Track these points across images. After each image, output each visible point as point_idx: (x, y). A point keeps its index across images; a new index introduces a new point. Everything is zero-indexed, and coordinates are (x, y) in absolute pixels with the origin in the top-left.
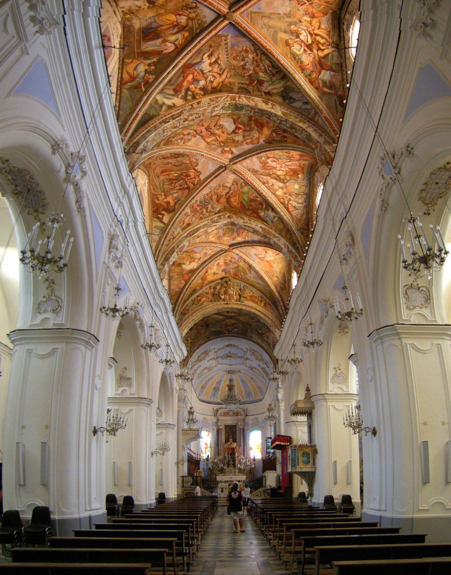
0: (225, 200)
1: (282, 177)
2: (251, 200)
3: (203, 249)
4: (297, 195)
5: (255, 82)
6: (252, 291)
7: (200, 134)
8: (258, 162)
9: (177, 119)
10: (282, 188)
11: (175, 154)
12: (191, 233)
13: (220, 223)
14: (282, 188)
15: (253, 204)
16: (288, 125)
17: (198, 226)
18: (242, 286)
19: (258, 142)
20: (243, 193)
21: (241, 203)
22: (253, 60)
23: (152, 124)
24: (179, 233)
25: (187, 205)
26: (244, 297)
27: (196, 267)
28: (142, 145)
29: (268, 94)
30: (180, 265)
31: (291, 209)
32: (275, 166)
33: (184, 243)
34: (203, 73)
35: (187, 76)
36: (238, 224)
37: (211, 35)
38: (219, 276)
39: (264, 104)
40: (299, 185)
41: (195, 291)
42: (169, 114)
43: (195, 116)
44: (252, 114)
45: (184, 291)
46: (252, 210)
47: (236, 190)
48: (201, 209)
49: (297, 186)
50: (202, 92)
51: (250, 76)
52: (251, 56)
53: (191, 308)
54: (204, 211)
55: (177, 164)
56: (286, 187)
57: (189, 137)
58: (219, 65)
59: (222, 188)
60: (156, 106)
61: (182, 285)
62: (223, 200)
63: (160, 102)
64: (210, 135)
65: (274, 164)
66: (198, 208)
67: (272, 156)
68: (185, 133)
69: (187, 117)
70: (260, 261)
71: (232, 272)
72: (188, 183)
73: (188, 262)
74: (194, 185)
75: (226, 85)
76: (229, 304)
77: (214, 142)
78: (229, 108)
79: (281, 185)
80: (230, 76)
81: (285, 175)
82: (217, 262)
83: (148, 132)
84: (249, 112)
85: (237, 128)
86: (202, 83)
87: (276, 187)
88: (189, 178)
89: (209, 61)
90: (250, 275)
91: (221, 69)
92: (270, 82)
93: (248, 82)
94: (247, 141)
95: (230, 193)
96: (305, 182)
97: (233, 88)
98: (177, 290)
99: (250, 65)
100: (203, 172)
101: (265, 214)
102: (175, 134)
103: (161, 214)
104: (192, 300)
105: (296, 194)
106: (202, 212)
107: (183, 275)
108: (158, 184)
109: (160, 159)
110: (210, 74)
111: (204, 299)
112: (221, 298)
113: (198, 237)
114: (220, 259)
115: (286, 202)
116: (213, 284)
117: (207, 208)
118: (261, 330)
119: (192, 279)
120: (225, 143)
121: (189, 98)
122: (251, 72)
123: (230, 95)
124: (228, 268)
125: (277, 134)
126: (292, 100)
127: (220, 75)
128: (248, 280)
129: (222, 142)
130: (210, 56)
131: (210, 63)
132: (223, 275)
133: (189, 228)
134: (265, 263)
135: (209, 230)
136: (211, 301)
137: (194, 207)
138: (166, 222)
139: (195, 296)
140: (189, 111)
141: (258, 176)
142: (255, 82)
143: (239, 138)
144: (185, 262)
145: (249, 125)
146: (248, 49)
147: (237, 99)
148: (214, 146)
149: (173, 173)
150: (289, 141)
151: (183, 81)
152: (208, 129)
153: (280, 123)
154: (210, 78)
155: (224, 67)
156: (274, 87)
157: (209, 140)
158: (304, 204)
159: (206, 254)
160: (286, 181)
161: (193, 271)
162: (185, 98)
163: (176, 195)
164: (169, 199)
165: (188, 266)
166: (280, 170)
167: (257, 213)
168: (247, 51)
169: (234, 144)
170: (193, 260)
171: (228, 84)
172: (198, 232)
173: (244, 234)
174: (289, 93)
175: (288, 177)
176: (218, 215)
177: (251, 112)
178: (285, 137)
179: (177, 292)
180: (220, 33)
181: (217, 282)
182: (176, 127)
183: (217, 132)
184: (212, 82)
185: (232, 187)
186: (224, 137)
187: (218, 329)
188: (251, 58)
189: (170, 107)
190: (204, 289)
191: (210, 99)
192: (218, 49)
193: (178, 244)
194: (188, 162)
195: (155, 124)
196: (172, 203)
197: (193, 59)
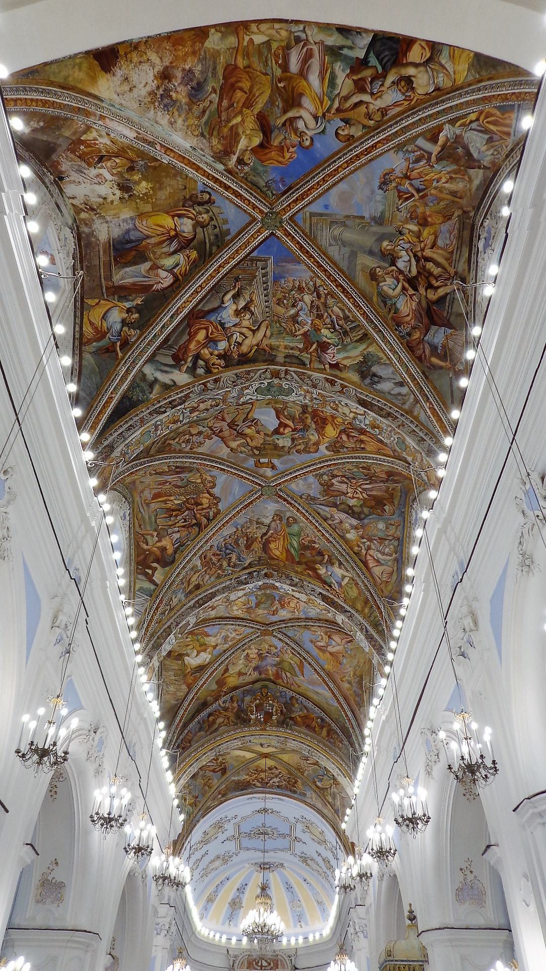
1: (356, 509)
2: (304, 547)
3: (221, 628)
5: (314, 346)
7: (219, 434)
9: (180, 407)
10: (356, 528)
11: (177, 467)
12: (201, 602)
13: (251, 586)
15: (308, 553)
16: (367, 422)
17: (213, 590)
19: (317, 451)
21: (288, 551)
22: (312, 307)
23: (137, 415)
25: (195, 554)
26: (292, 719)
28: (119, 449)
29: (336, 366)
30: (180, 657)
31: (371, 564)
33: (188, 618)
34: (224, 328)
35: (196, 333)
36: (282, 588)
37: (238, 258)
38: (248, 679)
39: (327, 385)
40: (386, 523)
41: (205, 705)
42: (165, 399)
43: (210, 402)
44: (307, 401)
46: (306, 563)
48: (219, 561)
49: (381, 526)
50: (222, 362)
51: (305, 335)
52: (307, 298)
53: (196, 738)
54: (225, 564)
55: (179, 484)
56: (363, 527)
57: (201, 439)
58: (253, 314)
59: (255, 526)
60: (142, 384)
61: (181, 694)
62: (257, 546)
63: (150, 378)
64: (237, 436)
65: (343, 487)
68: (194, 431)
69: (196, 405)
71: (271, 671)
72: (198, 515)
73: (195, 652)
74: (208, 519)
75: (264, 350)
77: (243, 449)
78: (269, 390)
79: (354, 522)
80: (272, 335)
81: (361, 506)
83: (129, 429)
84: (301, 398)
85: (282, 425)
86: (222, 345)
88: (199, 507)
89: (234, 307)
91: (255, 322)
92: (339, 347)
93: (301, 346)
94: (298, 447)
95: (269, 534)
97: (276, 356)
99: (306, 314)
100: (223, 499)
101: (327, 571)
102: (177, 434)
103: (150, 568)
104: (199, 722)
105: (380, 538)
106: (221, 565)
108: (147, 517)
109: (151, 474)
110: (237, 329)
111: (220, 720)
112: (250, 720)
113: (213, 608)
114: (249, 648)
115: (364, 552)
117: (230, 558)
118: (321, 780)
120: (261, 450)
121: (200, 371)
122: (307, 328)
123: (270, 367)
124: (264, 663)
125: (348, 436)
126: (376, 379)
127: (254, 332)
128: (299, 686)
129: (256, 448)
130: (236, 297)
131: (236, 310)
132: (255, 675)
133: (198, 592)
135: (233, 597)
137: (208, 557)
139: (204, 714)
140: (200, 394)
141: (315, 507)
142: (314, 346)
143: (284, 442)
144: (189, 651)
145: (302, 420)
146: (304, 285)
147: (283, 375)
149: (172, 498)
150: (368, 448)
151: (189, 341)
152: (232, 425)
153: (354, 418)
154: (237, 337)
155: (260, 318)
156: (346, 355)
157: (234, 445)
158: (394, 556)
159: (225, 638)
160: (363, 516)
161: (201, 668)
162: (192, 370)
163: (176, 536)
164: (166, 542)
165: (194, 660)
166: (353, 498)
167: (315, 570)
168: (300, 289)
169: (276, 452)
170: (203, 648)
171: (267, 348)
172: (213, 600)
173: (292, 605)
174: (371, 366)
175: (366, 510)
176: (247, 571)
177: (305, 397)
178: (362, 442)
180: (254, 254)
182: (178, 421)
183: (248, 431)
184: (240, 344)
185: (273, 524)
186: (258, 441)
187: (244, 777)
188: (309, 302)
189: (166, 387)
190: (221, 702)
191: (236, 374)
192: (250, 285)
193: (178, 620)
194: (199, 481)
195: (141, 416)
196: (170, 550)
197: (207, 302)
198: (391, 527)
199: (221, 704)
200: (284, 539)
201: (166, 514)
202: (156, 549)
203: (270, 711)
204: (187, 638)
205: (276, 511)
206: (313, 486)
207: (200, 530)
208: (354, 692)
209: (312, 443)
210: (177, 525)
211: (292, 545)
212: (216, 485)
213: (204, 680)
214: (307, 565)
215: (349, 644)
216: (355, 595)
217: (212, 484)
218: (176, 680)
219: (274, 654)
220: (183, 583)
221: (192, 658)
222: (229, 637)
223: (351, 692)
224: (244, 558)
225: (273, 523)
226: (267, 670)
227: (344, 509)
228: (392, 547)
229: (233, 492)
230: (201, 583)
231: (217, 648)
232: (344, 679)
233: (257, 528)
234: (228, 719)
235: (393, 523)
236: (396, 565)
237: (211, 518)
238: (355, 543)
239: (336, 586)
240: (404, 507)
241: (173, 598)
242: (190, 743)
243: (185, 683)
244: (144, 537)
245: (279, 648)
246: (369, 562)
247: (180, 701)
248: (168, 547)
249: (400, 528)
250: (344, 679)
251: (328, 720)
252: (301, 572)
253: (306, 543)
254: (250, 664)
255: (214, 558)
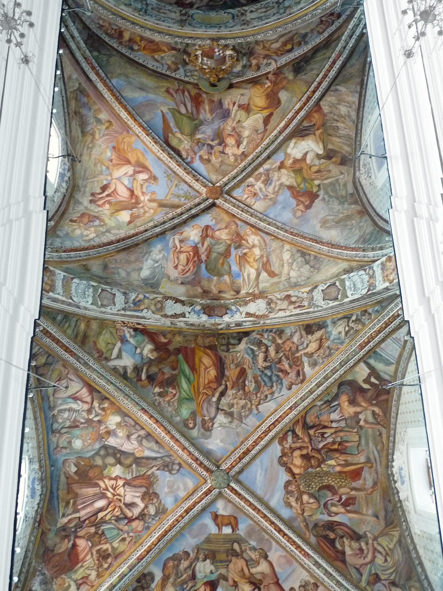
0: (227, 373)
1: (111, 460)
4: (75, 426)
6: (156, 60)
8: (162, 496)
10: (109, 433)
14: (109, 433)
15: (168, 372)
18: (181, 71)
20: (190, 399)
21: (193, 369)
24: (334, 323)
27: (292, 144)
31: (84, 393)
32: (128, 489)
40: (72, 448)
45: (325, 85)
46: (168, 353)
47: (205, 405)
48: (280, 361)
49: (78, 444)
56: (100, 437)
59: (235, 410)
61: (330, 98)
64: (261, 582)
66: (286, 365)
67: (135, 524)
70: (142, 159)
72: (306, 439)
73: (308, 161)
74: (294, 432)
76: (213, 39)
79: (112, 441)
81: (105, 466)
82: (242, 148)
87: (121, 433)
88: (304, 452)
90: (165, 110)
95: (217, 395)
96: (60, 457)
98: (342, 89)
101: (141, 353)
103: (372, 384)
104: (306, 43)
105: (77, 426)
106: (277, 352)
107: (324, 125)
108: (371, 445)
115: (96, 404)
116: (251, 74)
119: (302, 113)
124: (215, 125)
129: (236, 555)
134: (133, 161)
136: (257, 43)
138: (362, 365)
139: (298, 53)
144: (317, 162)
148: (253, 543)
149: (338, 469)
158: (55, 412)
159: (267, 182)
160: (102, 452)
163: (335, 416)
164: (351, 410)
166: (116, 478)
170: (298, 166)
173: (183, 257)
175: (99, 461)
179: (345, 81)
181: (241, 79)
190: (273, 67)
196: (344, 399)
198: (65, 444)
199: (273, 63)
200: (198, 389)
201: (347, 447)
202: (363, 404)
203: (205, 59)
204: (319, 186)
205: (210, 436)
206: (166, 490)
207: (304, 418)
208: (90, 109)
209: (171, 580)
210: (333, 431)
211: (188, 380)
212: (285, 486)
213: (299, 117)
214: (168, 351)
215: (105, 182)
216: (101, 338)
217: (290, 488)
218: (337, 121)
219: (204, 145)
220: (328, 348)
221: (312, 150)
222: (263, 182)
223: (96, 107)
224: (248, 354)
225: (212, 415)
226: (212, 111)
227: (126, 458)
228: (60, 421)
229: (264, 472)
230: (303, 333)
231: (278, 164)
232: (107, 124)
233: (233, 405)
234: (264, 47)
235: (64, 451)
236: (52, 403)
237: (290, 433)
238: (108, 412)
239: (128, 335)
240: (52, 472)
241: (343, 333)
242: (322, 21)
243: (324, 115)
244: (377, 421)
245: (197, 158)
246: (87, 394)
247: (332, 88)
248: (346, 403)
249: (52, 447)
250: (107, 124)
251: (124, 51)
252: (174, 335)
253: (170, 390)
254: (234, 124)
255: (287, 367)
